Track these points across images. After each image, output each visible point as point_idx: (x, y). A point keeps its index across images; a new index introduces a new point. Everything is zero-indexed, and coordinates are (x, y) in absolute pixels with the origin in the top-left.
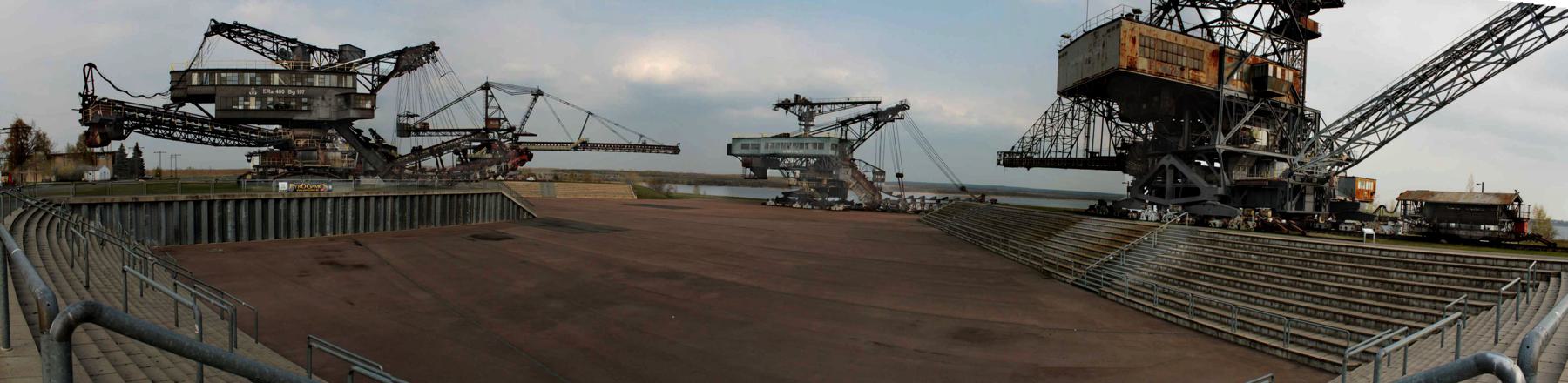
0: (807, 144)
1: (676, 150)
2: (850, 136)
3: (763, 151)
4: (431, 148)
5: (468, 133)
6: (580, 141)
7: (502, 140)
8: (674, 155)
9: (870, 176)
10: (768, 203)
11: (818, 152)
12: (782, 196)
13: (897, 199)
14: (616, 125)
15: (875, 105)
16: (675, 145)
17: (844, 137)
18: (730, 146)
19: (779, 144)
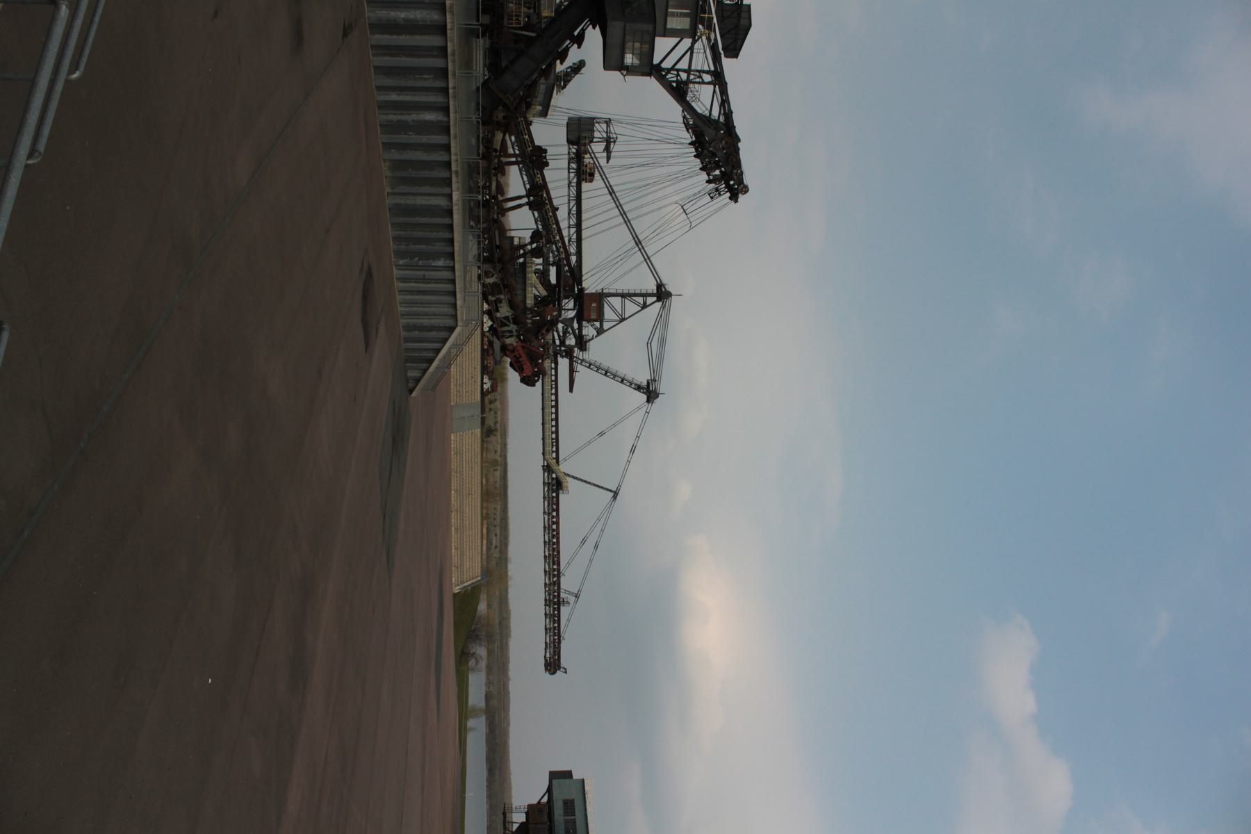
1: (553, 665)
4: (544, 186)
5: (574, 259)
6: (561, 475)
7: (560, 326)
8: (543, 662)
14: (596, 546)
16: (563, 663)
18: (568, 775)
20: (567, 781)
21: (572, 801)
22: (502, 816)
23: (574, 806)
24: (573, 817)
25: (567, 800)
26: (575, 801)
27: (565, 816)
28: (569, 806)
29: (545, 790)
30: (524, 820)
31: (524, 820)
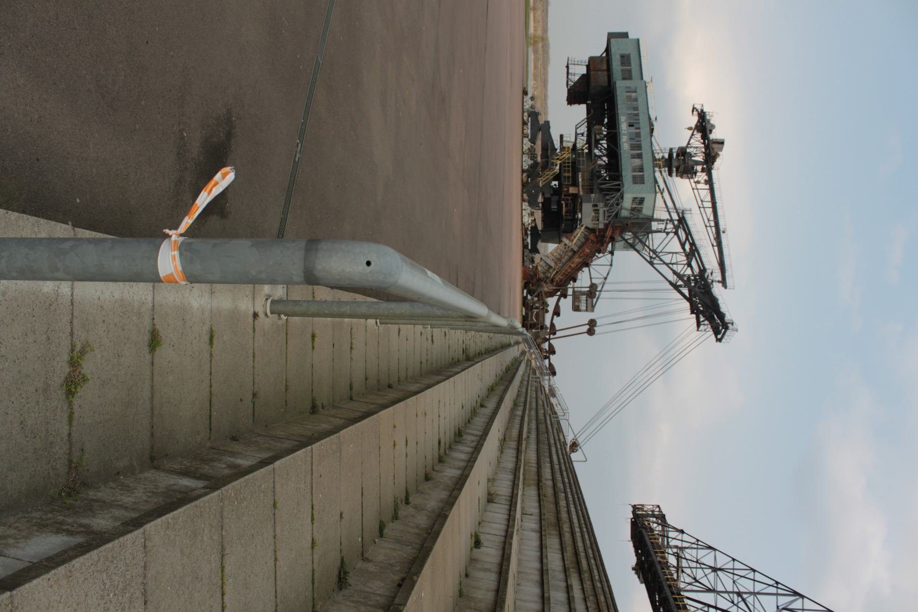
0: (640, 156)
2: (656, 240)
3: (621, 86)
9: (583, 280)
10: (527, 98)
11: (627, 174)
12: (541, 122)
15: (720, 278)
17: (655, 226)
18: (625, 35)
19: (636, 109)
20: (624, 40)
21: (628, 56)
22: (566, 69)
24: (629, 68)
26: (631, 57)
27: (622, 66)
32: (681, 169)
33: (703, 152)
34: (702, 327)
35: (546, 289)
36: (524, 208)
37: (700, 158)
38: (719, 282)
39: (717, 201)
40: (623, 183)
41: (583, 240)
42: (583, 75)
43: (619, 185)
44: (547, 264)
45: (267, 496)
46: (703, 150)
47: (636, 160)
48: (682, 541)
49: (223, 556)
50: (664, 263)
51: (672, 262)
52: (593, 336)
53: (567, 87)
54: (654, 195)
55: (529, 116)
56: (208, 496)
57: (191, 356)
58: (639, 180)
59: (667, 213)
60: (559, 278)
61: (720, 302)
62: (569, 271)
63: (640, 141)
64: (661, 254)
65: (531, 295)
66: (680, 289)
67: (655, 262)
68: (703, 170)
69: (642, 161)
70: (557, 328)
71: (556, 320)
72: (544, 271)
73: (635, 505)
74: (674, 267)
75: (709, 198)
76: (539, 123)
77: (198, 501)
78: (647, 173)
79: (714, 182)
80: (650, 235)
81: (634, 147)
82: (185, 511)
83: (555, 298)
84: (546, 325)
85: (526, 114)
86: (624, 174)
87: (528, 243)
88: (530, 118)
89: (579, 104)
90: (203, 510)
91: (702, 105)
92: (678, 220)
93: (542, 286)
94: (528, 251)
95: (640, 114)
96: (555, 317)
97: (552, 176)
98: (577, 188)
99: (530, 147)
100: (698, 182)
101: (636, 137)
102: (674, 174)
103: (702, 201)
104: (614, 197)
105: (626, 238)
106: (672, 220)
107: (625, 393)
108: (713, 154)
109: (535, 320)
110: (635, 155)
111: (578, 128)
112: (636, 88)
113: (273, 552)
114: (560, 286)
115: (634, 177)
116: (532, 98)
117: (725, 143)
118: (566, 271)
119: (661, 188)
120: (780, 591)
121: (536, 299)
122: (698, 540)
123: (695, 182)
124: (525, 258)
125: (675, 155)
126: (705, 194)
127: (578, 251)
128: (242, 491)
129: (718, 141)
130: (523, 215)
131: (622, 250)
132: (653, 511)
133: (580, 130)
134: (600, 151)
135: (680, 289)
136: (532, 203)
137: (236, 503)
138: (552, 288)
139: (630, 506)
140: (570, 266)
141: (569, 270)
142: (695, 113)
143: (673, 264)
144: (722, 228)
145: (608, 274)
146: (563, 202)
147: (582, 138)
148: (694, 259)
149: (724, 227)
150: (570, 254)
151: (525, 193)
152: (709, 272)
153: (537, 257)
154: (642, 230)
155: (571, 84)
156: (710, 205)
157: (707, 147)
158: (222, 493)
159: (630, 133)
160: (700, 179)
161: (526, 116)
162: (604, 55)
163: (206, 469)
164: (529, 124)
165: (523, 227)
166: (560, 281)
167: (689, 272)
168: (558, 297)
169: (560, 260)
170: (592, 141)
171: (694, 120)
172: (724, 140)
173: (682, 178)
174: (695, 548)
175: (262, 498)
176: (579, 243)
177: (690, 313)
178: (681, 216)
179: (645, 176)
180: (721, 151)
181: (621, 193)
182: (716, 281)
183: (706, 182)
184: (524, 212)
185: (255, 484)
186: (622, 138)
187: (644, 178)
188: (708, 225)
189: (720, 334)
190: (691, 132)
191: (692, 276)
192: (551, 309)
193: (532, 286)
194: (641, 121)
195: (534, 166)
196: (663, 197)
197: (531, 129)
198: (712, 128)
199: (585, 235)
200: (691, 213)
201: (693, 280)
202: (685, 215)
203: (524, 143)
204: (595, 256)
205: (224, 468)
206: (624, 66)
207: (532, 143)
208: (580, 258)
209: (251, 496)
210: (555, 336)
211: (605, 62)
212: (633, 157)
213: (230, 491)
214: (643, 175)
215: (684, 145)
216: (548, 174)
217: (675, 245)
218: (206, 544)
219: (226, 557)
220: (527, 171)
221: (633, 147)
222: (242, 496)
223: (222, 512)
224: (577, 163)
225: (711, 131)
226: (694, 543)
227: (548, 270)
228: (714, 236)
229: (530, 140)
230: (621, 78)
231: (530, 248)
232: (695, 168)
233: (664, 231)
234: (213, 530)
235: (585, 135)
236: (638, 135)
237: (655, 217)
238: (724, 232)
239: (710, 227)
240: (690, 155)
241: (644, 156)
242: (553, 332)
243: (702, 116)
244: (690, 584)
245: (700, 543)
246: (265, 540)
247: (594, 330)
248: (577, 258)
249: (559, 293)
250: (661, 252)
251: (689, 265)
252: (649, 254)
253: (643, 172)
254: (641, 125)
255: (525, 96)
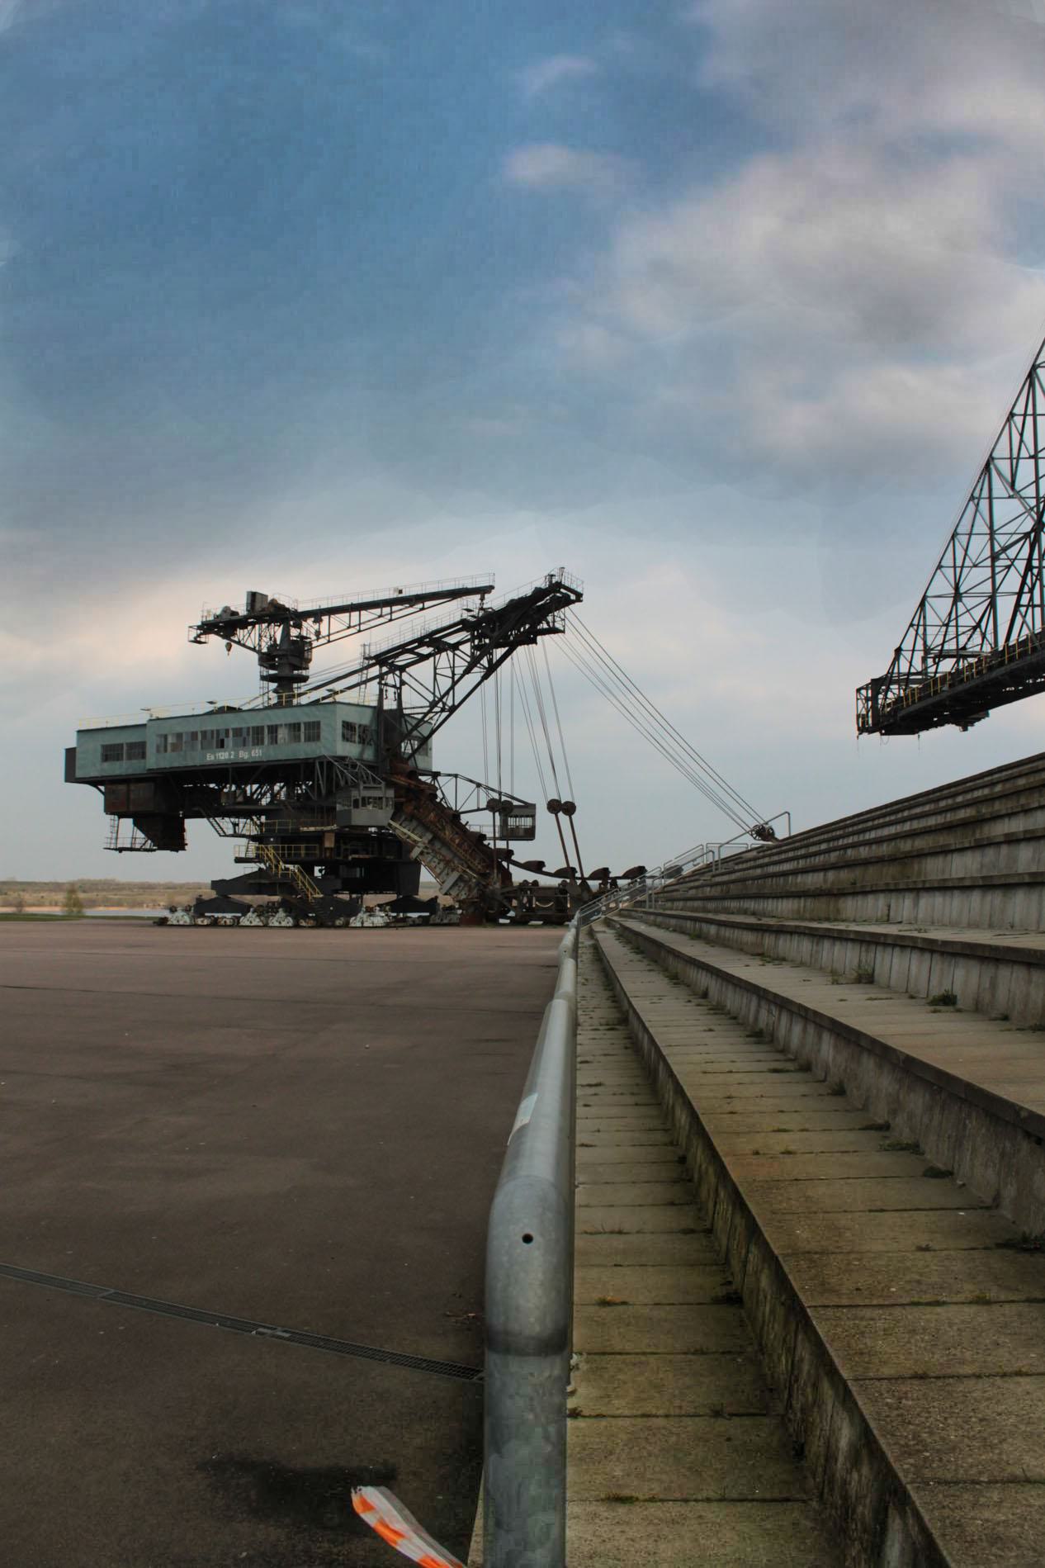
0: (273, 729)
2: (414, 701)
3: (154, 761)
9: (482, 823)
10: (173, 919)
11: (304, 750)
12: (213, 894)
13: (555, 882)
15: (479, 596)
17: (390, 704)
18: (71, 754)
19: (194, 735)
20: (78, 755)
23: (111, 746)
24: (125, 748)
25: (102, 755)
28: (111, 753)
29: (94, 789)
30: (130, 821)
31: (130, 821)
32: (295, 661)
33: (268, 627)
34: (558, 625)
35: (498, 886)
36: (359, 925)
37: (278, 632)
38: (482, 599)
39: (349, 603)
40: (319, 757)
41: (414, 823)
42: (135, 824)
43: (321, 764)
44: (455, 884)
45: (906, 1393)
46: (264, 625)
47: (280, 736)
48: (913, 650)
49: (1028, 1481)
50: (452, 688)
51: (451, 675)
52: (576, 804)
53: (154, 850)
54: (338, 706)
55: (202, 915)
56: (922, 1510)
57: (656, 1541)
58: (313, 731)
59: (368, 684)
60: (479, 864)
61: (515, 596)
62: (466, 848)
63: (248, 728)
64: (437, 694)
65: (509, 911)
66: (494, 661)
67: (450, 703)
68: (299, 626)
69: (281, 725)
70: (565, 866)
71: (550, 867)
72: (466, 889)
73: (859, 729)
74: (459, 671)
75: (345, 616)
76: (215, 899)
77: (933, 1531)
78: (303, 717)
79: (318, 608)
80: (406, 712)
81: (258, 740)
82: (954, 1561)
83: (512, 869)
84: (559, 885)
85: (199, 921)
86: (302, 756)
87: (420, 917)
88: (207, 914)
89: (184, 830)
90: (948, 1521)
91: (190, 627)
92: (381, 667)
93: (493, 892)
94: (433, 916)
95: (204, 729)
96: (544, 869)
97: (305, 877)
98: (327, 835)
99: (256, 914)
100: (318, 633)
101: (241, 735)
102: (304, 673)
103: (349, 627)
104: (342, 772)
105: (410, 752)
106: (381, 676)
107: (671, 751)
108: (272, 610)
109: (552, 903)
110: (272, 738)
111: (224, 832)
112: (160, 736)
113: (1006, 1379)
114: (493, 861)
115: (309, 739)
116: (173, 910)
117: (254, 591)
118: (466, 851)
119: (328, 693)
120: (985, 493)
121: (515, 903)
122: (911, 625)
123: (318, 639)
124: (445, 921)
125: (272, 672)
126: (338, 622)
127: (432, 832)
128: (902, 1442)
129: (249, 602)
130: (371, 925)
131: (431, 757)
132: (867, 699)
133: (227, 828)
134: (263, 795)
135: (494, 661)
136: (352, 909)
137: (928, 1454)
138: (495, 875)
139: (861, 736)
140: (458, 845)
141: (466, 846)
142: (203, 639)
143: (454, 674)
144: (394, 595)
145: (471, 781)
146: (350, 858)
147: (241, 825)
148: (445, 640)
149: (392, 592)
150: (438, 845)
151: (334, 922)
152: (466, 615)
153: (445, 901)
154: (398, 726)
155: (149, 844)
156: (355, 614)
157: (260, 620)
158: (912, 1482)
159: (236, 745)
160: (313, 631)
161: (202, 922)
162: (102, 788)
163: (864, 1511)
164: (216, 915)
165: (393, 925)
166: (484, 862)
167: (466, 648)
168: (511, 866)
169: (448, 863)
170: (247, 809)
171: (215, 641)
172: (248, 593)
173: (310, 660)
174: (925, 630)
175: (910, 1403)
176: (420, 830)
177: (534, 645)
178: (374, 661)
179: (307, 720)
180: (266, 596)
181: (336, 761)
182: (482, 604)
183: (318, 620)
184: (366, 924)
185: (888, 1416)
186: (243, 758)
187: (309, 723)
188: (389, 617)
189: (569, 596)
190: (233, 644)
191: (474, 642)
192: (531, 877)
193: (492, 909)
194: (215, 728)
195: (289, 908)
196: (342, 691)
197: (224, 912)
198: (230, 612)
199: (405, 820)
200: (369, 645)
201: (480, 641)
202: (373, 655)
203: (248, 923)
204: (440, 803)
205: (860, 1476)
206: (122, 754)
207: (249, 912)
208: (444, 829)
209: (909, 1423)
210: (578, 869)
211: (114, 787)
212: (274, 740)
213: (906, 1466)
214: (305, 723)
215: (255, 656)
216: (303, 883)
217: (423, 671)
218: (1011, 1517)
219: (1029, 1474)
220: (294, 918)
221: (258, 741)
222: (912, 1443)
223: (947, 1483)
224: (282, 834)
225: (234, 613)
226: (917, 631)
227: (466, 882)
228: (406, 608)
229: (244, 915)
230: (143, 761)
231: (427, 914)
232: (295, 639)
233: (399, 689)
234: (982, 1500)
235: (237, 820)
236: (238, 732)
237: (375, 704)
238: (400, 592)
239: (391, 613)
240: (273, 647)
241: (274, 723)
242: (570, 870)
243: (207, 628)
244: (984, 636)
245: (915, 622)
246: (986, 1395)
247: (567, 803)
248: (445, 834)
249: (505, 864)
250: (434, 694)
251: (455, 647)
252: (437, 713)
253: (299, 724)
254: (222, 727)
255: (169, 923)
